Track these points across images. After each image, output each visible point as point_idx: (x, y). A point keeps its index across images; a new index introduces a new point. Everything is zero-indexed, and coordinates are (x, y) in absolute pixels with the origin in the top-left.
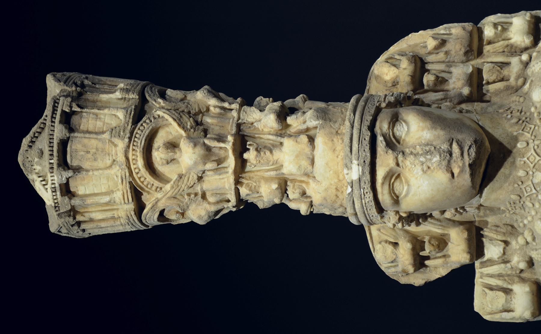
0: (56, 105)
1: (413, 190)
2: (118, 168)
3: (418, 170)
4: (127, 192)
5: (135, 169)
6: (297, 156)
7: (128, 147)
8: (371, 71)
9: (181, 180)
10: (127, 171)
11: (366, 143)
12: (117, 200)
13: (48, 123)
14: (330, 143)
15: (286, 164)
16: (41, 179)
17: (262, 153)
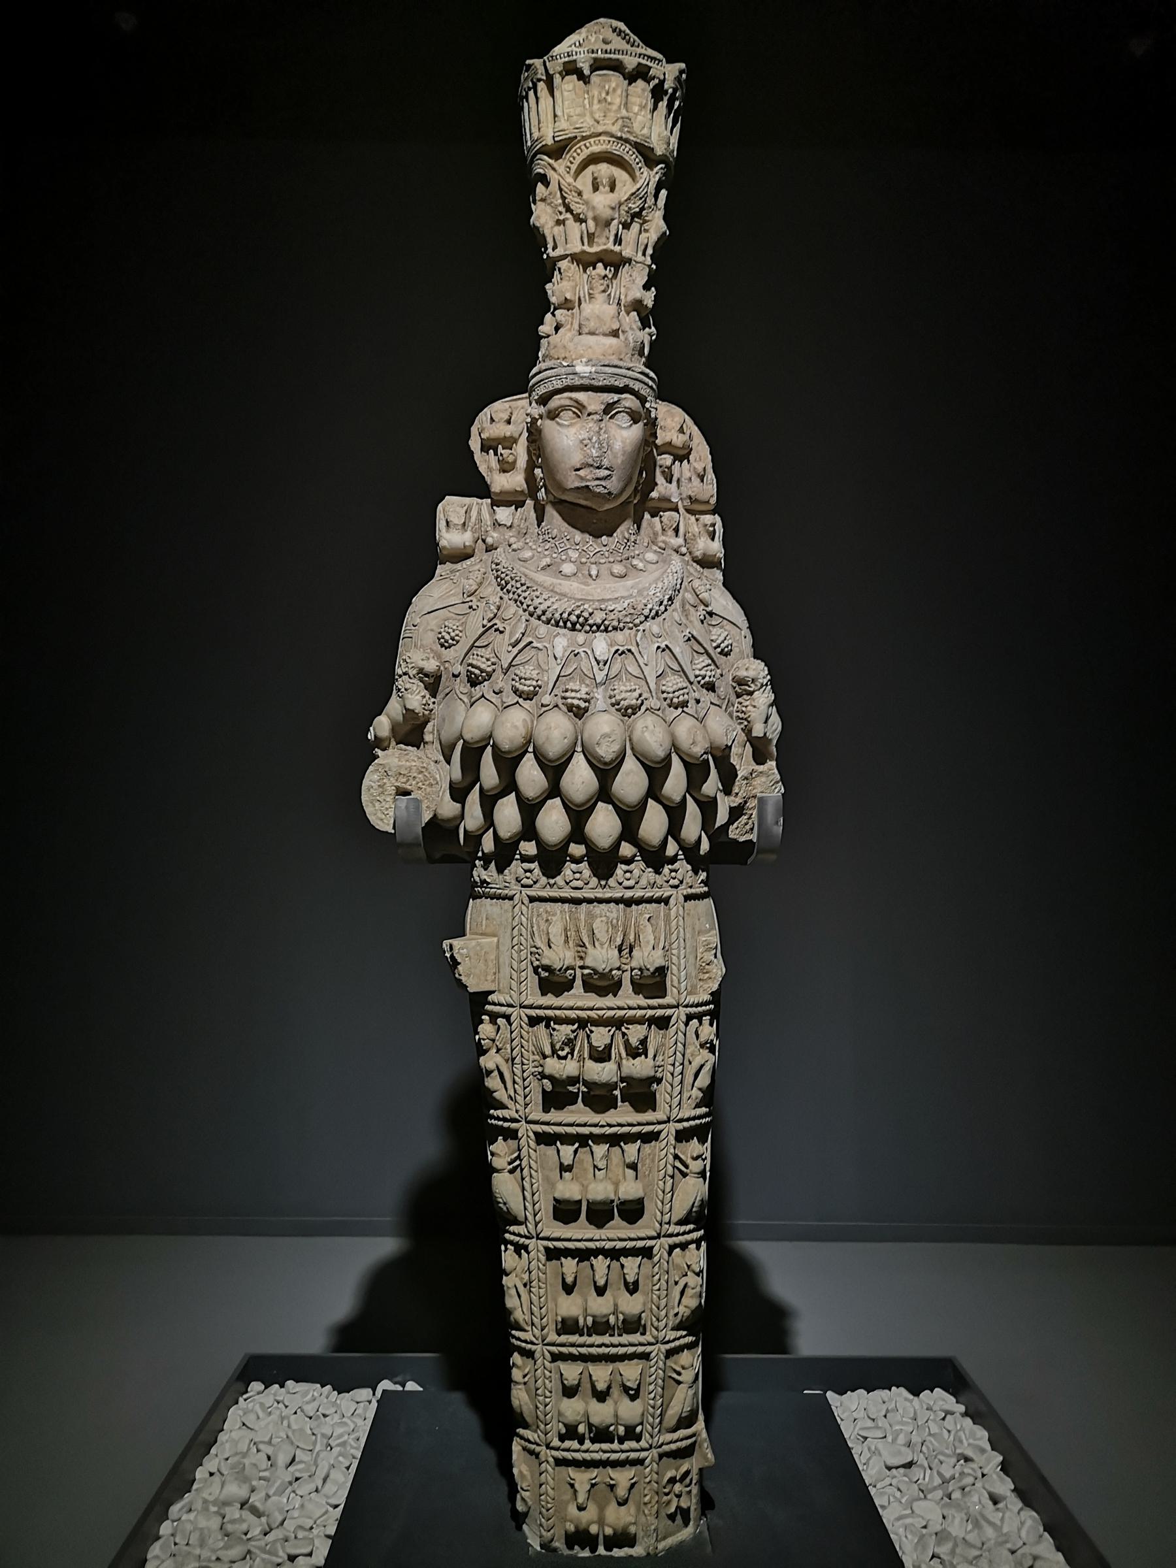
1: (565, 431)
3: (584, 435)
7: (612, 136)
13: (639, 50)
15: (591, 306)
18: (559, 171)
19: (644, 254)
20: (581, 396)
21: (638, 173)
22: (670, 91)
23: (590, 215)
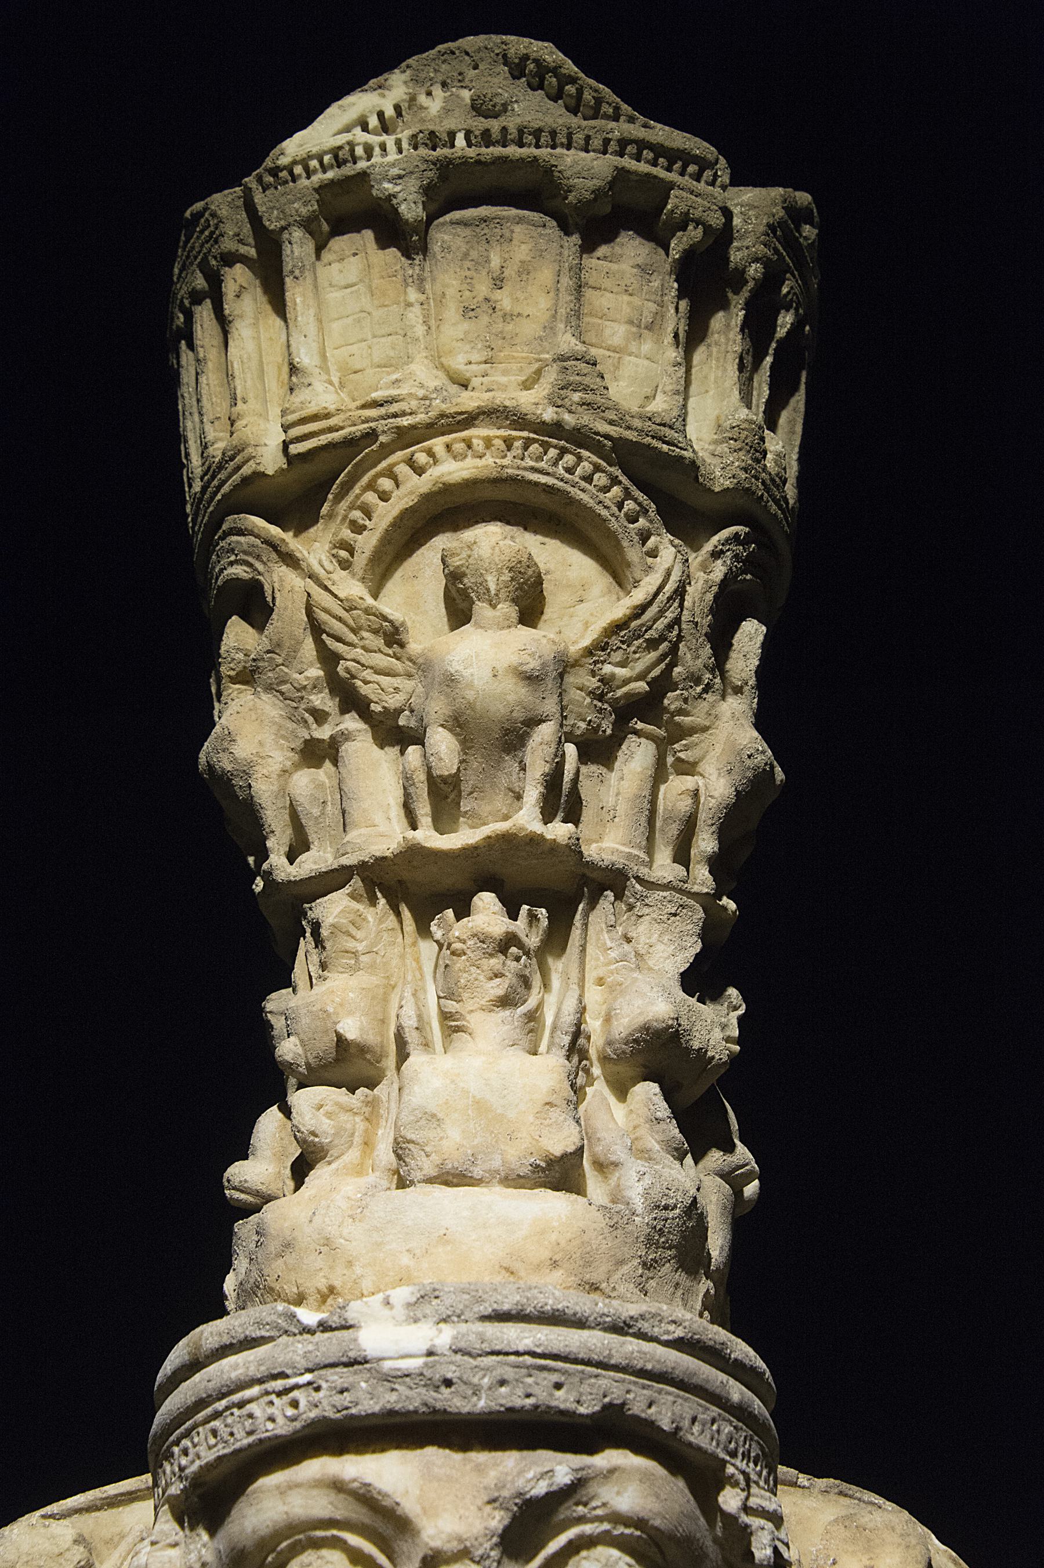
0: (692, 168)
2: (432, 384)
4: (331, 430)
5: (430, 453)
6: (480, 1107)
7: (518, 420)
8: (880, 1501)
9: (379, 642)
10: (421, 418)
11: (537, 1391)
12: (298, 398)
13: (621, 129)
14: (545, 1254)
16: (390, 112)
17: (496, 962)
18: (312, 570)
19: (682, 856)
20: (389, 1472)
21: (633, 554)
22: (755, 270)
23: (437, 708)
